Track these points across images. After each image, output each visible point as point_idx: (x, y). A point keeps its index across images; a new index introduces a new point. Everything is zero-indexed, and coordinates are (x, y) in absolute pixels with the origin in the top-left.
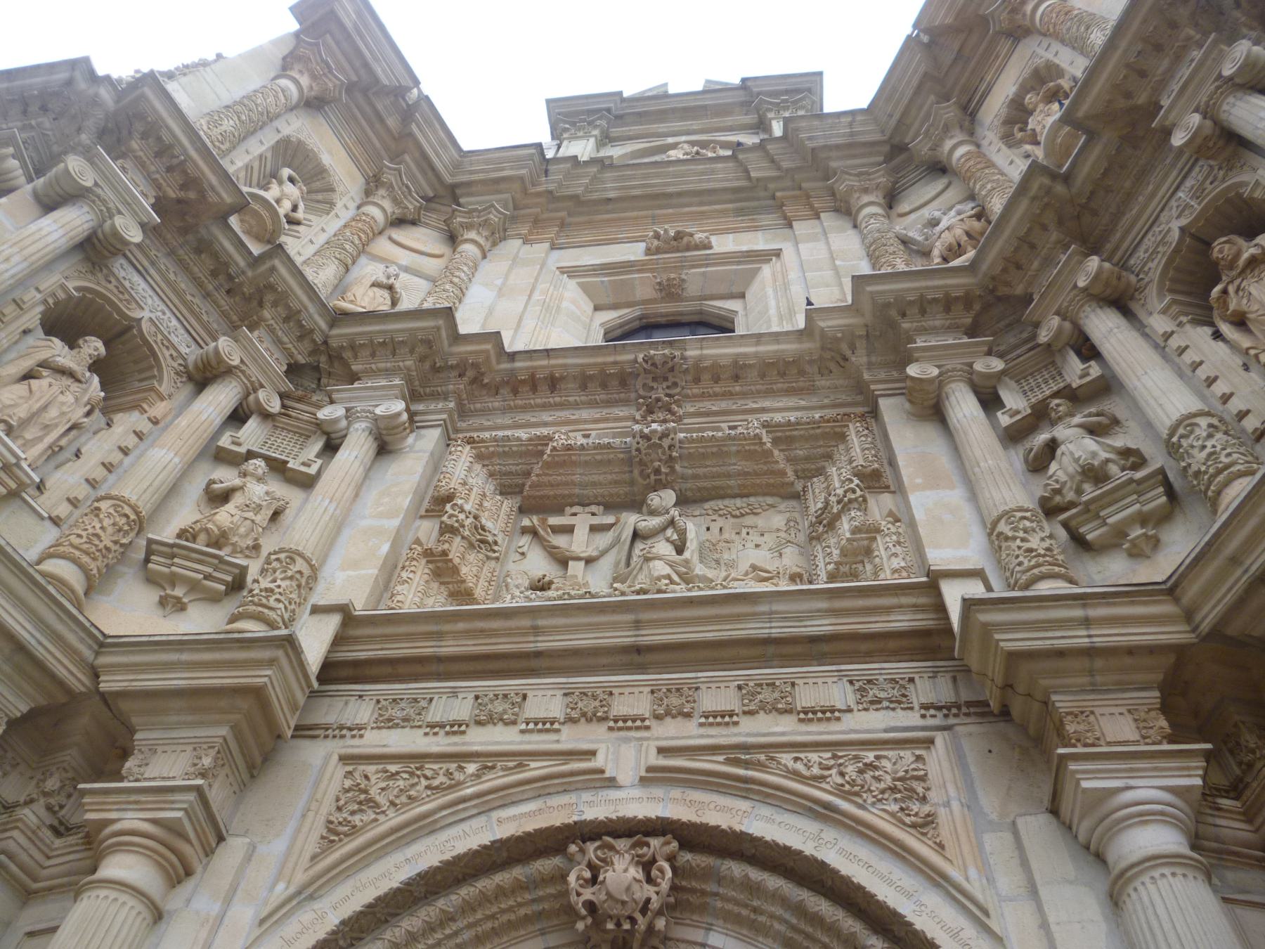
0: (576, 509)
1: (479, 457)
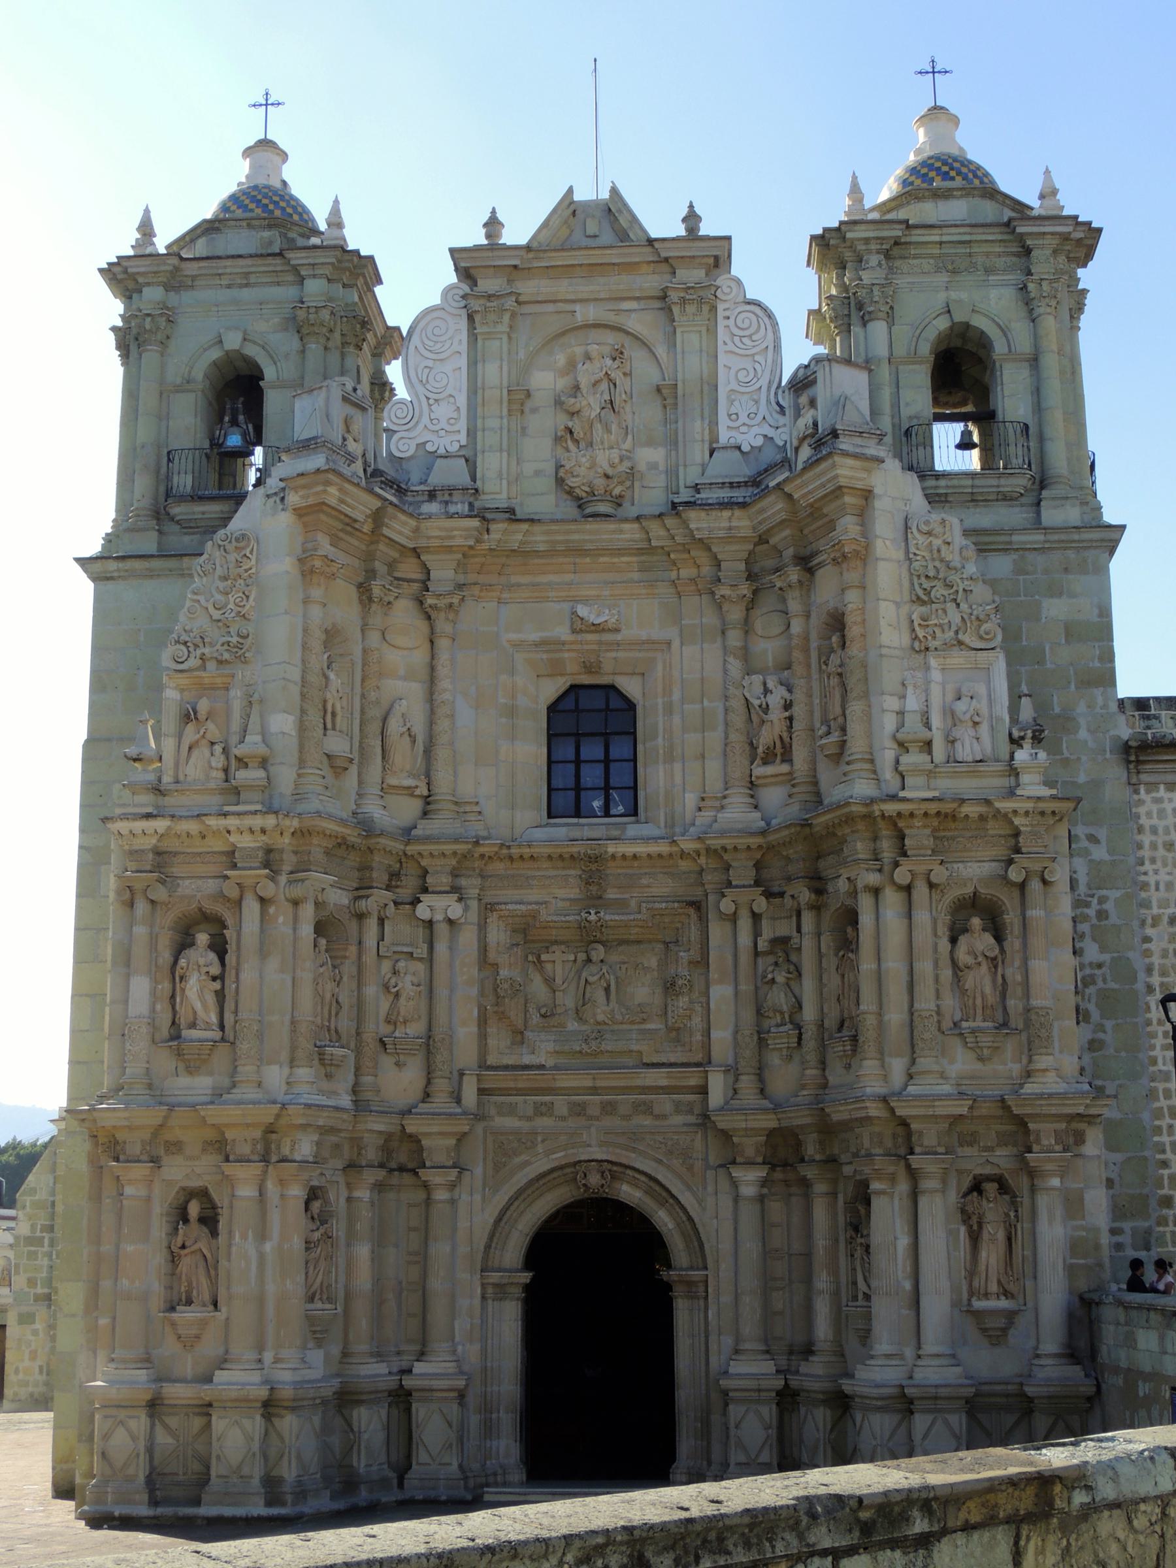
0: (555, 948)
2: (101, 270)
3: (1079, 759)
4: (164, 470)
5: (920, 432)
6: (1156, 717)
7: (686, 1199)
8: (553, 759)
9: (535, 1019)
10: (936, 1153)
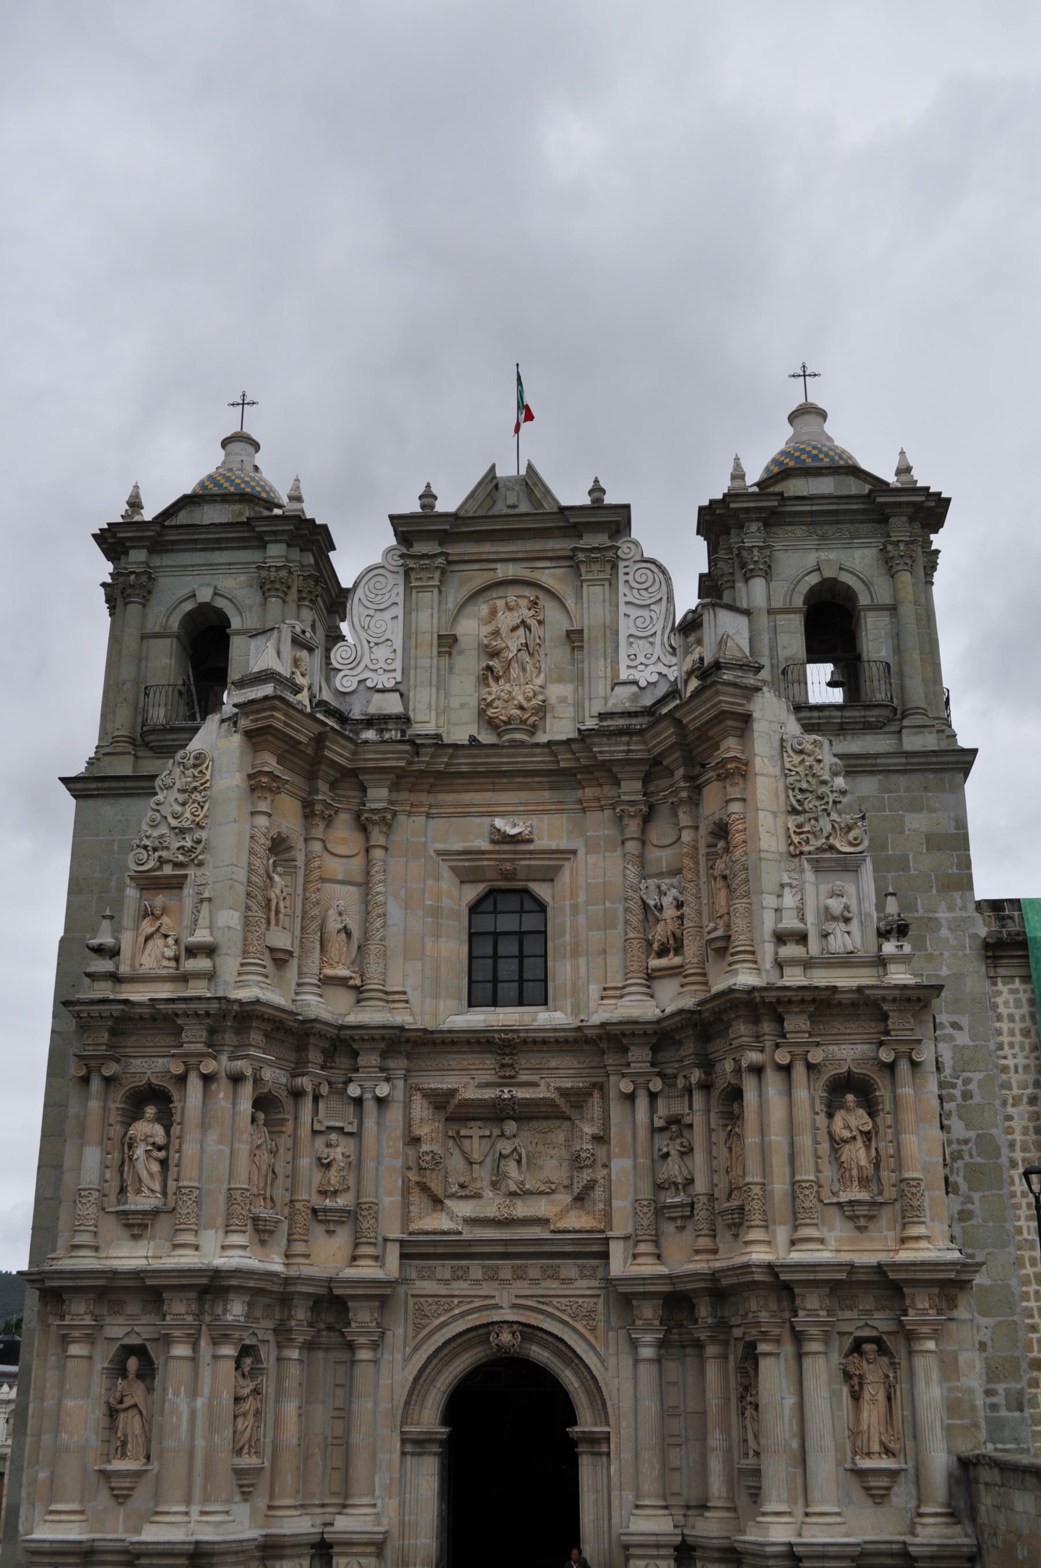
0: (471, 1124)
1: (425, 1096)
2: (94, 536)
3: (941, 954)
4: (141, 704)
5: (795, 670)
6: (1011, 918)
7: (590, 1358)
8: (474, 955)
9: (455, 1188)
10: (818, 1315)
